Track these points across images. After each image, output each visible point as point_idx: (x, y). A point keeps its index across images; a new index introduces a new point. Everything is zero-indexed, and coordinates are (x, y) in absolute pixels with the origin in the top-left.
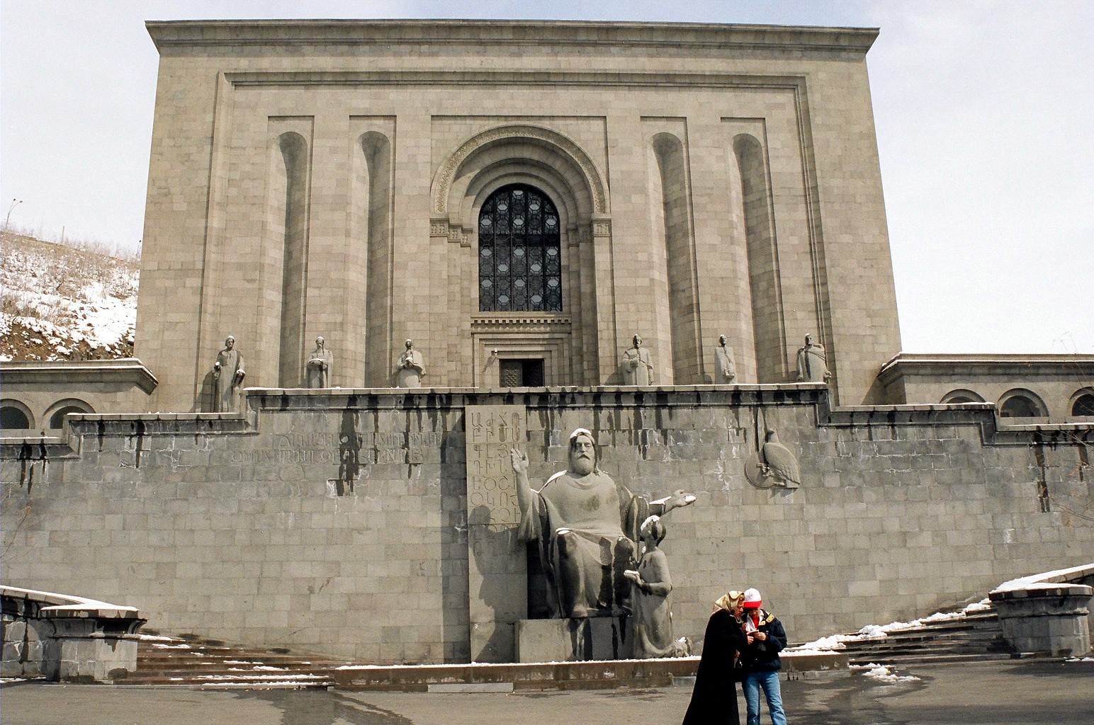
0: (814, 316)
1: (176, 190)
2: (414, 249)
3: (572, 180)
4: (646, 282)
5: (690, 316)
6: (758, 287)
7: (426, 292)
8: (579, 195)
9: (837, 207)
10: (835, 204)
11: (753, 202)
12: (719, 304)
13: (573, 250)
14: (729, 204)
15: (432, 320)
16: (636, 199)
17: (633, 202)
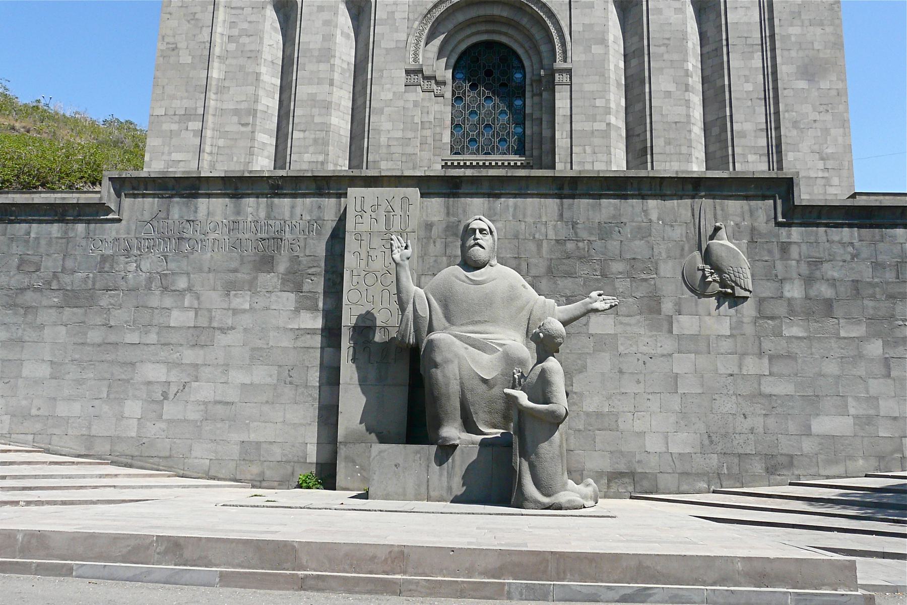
0: (765, 159)
1: (182, 45)
2: (390, 96)
3: (538, 35)
4: (603, 126)
5: (644, 157)
6: (711, 133)
7: (399, 134)
8: (544, 48)
9: (793, 54)
10: (791, 52)
11: (708, 53)
12: (672, 146)
13: (536, 99)
14: (686, 54)
15: (404, 159)
16: (597, 49)
17: (593, 52)
